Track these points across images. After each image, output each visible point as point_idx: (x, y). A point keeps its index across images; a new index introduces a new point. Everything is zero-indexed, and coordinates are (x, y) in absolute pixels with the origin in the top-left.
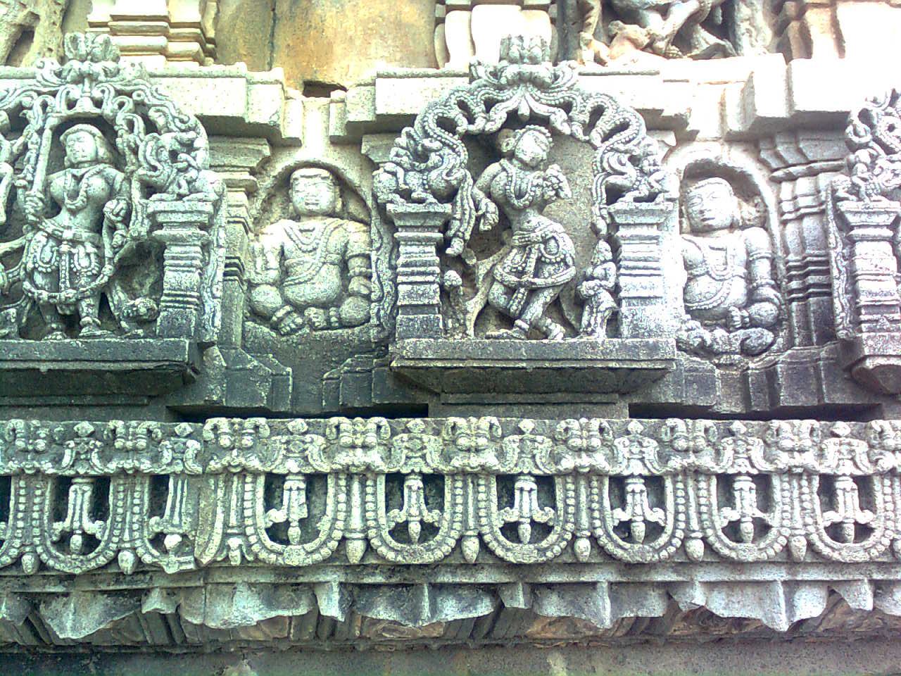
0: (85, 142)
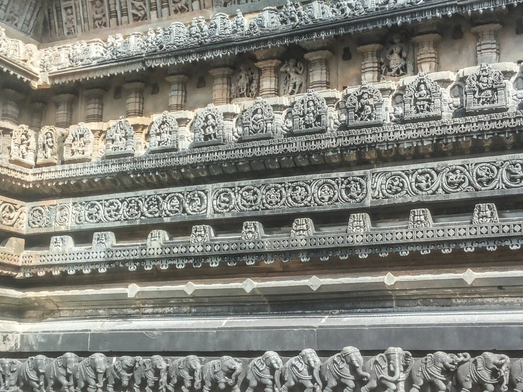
0: (311, 104)
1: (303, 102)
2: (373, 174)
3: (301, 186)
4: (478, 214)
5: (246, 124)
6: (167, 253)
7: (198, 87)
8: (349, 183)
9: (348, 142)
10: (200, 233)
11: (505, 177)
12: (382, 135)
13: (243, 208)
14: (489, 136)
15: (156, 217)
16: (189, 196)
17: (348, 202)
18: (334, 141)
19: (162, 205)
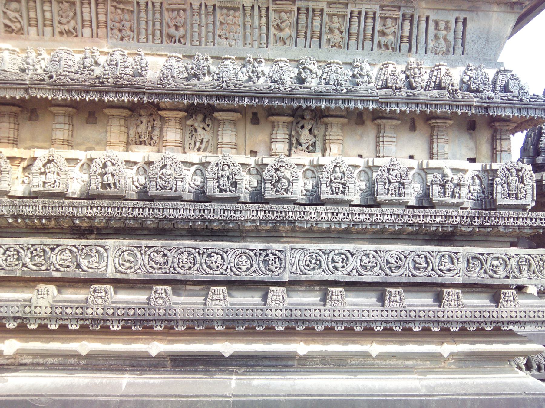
0: (226, 168)
1: (217, 164)
2: (292, 249)
3: (217, 254)
4: (390, 299)
5: (153, 178)
6: (58, 313)
7: (87, 123)
8: (267, 255)
9: (269, 216)
10: (99, 294)
11: (411, 265)
12: (304, 214)
13: (151, 270)
14: (399, 227)
15: (42, 270)
16: (85, 251)
17: (266, 274)
18: (255, 212)
19: (49, 258)
